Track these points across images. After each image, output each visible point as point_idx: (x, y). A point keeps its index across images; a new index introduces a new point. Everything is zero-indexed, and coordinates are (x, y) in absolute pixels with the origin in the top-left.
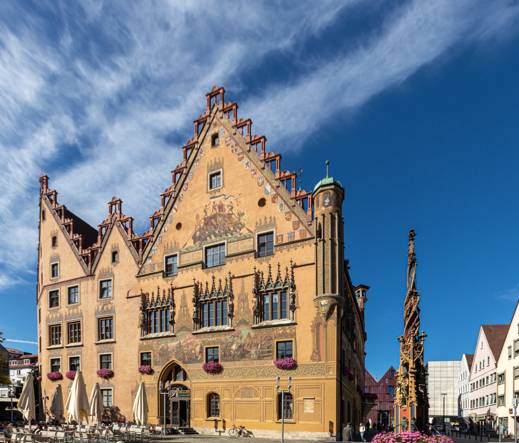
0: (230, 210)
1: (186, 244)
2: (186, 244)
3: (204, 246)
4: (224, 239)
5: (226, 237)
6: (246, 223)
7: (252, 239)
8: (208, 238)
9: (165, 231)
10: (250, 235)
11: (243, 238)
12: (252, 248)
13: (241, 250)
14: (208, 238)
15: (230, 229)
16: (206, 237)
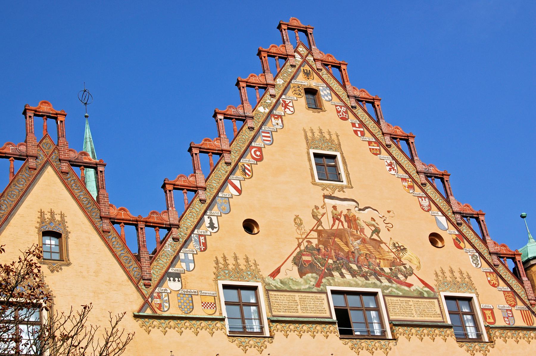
0: (373, 232)
1: (278, 271)
2: (278, 271)
3: (329, 289)
4: (375, 285)
5: (378, 282)
6: (414, 267)
7: (436, 301)
8: (336, 274)
9: (212, 226)
10: (426, 292)
11: (415, 294)
12: (440, 319)
13: (417, 318)
14: (336, 274)
15: (382, 269)
16: (329, 270)
